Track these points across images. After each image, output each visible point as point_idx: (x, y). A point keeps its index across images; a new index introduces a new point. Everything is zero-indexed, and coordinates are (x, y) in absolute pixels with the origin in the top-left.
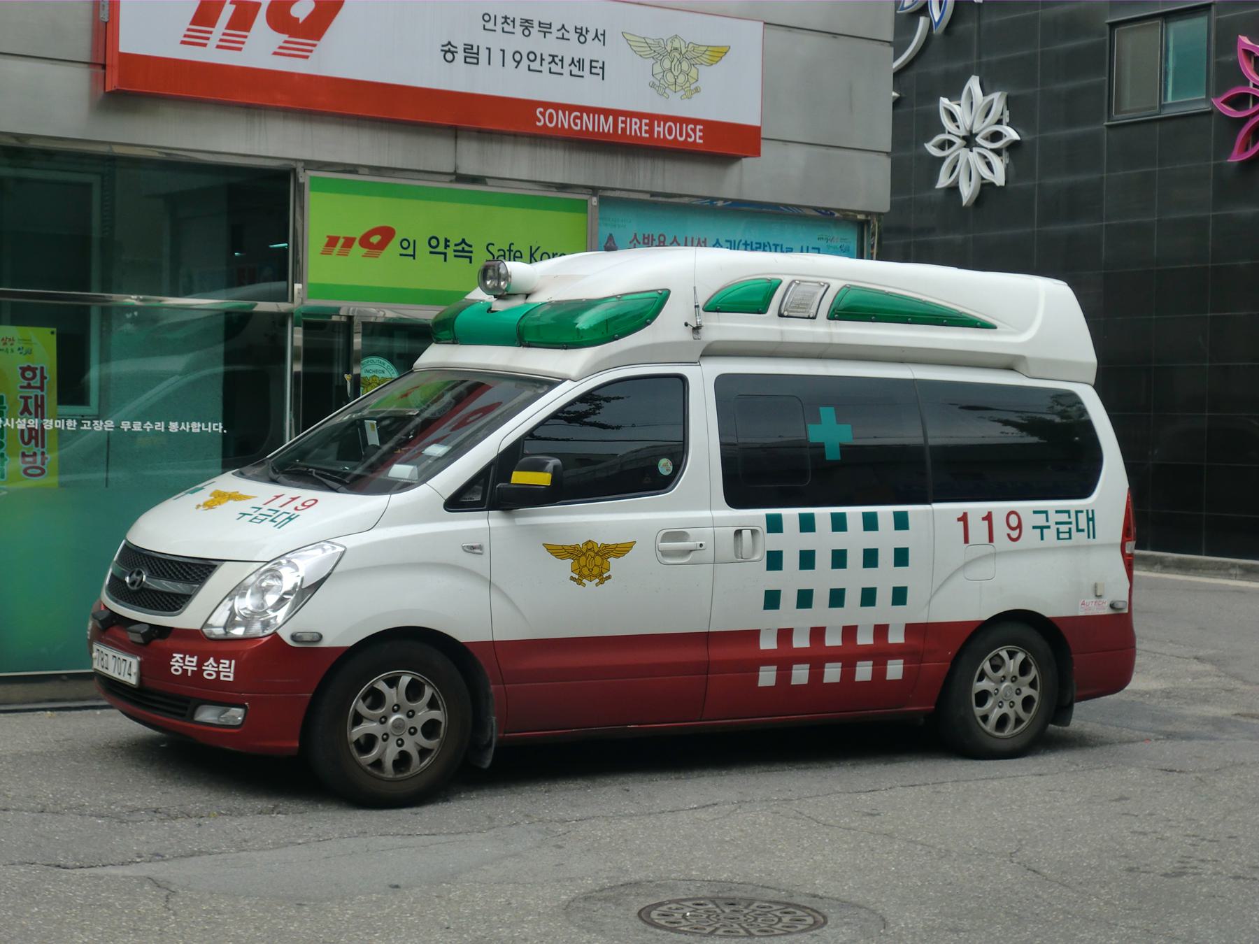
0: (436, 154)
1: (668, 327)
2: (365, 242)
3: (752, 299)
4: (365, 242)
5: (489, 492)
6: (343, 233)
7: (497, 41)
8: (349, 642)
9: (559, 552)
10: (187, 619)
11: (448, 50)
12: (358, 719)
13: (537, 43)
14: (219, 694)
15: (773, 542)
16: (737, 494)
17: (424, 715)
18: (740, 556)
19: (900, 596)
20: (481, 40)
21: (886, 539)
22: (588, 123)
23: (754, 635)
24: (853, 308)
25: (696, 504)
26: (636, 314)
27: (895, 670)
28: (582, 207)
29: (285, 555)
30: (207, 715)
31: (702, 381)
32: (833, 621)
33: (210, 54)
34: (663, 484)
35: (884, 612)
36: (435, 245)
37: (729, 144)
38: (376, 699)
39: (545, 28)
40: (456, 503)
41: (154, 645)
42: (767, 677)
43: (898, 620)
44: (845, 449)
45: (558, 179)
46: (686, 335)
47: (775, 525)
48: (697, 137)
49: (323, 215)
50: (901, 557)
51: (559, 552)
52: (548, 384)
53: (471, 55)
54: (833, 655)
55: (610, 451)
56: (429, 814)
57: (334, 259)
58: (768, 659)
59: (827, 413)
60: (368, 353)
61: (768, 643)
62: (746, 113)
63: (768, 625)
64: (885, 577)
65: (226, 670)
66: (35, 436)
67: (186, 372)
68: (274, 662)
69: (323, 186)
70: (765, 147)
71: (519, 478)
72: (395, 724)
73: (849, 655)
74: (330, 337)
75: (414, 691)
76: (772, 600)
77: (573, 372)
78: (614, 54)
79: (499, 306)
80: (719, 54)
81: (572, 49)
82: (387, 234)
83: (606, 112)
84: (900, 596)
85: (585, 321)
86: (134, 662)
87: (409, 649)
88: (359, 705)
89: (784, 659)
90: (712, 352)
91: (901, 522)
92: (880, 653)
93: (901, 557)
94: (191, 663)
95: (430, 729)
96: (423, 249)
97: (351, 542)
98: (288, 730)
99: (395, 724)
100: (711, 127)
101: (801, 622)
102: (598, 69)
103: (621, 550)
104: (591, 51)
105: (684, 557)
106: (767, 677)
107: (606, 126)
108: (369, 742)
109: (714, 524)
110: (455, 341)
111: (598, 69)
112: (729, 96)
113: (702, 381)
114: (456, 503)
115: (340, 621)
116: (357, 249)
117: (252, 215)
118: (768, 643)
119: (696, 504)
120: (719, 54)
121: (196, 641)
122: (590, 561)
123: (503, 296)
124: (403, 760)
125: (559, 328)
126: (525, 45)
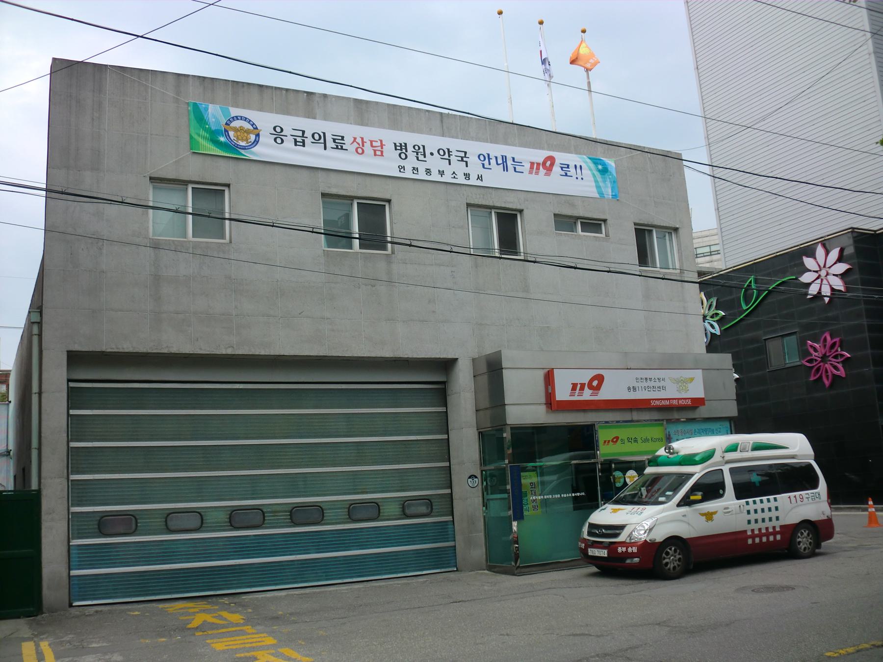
0: (627, 416)
1: (717, 458)
2: (612, 441)
3: (733, 448)
4: (612, 441)
5: (686, 502)
6: (607, 439)
7: (640, 384)
8: (661, 540)
9: (703, 515)
10: (621, 539)
11: (629, 389)
12: (664, 558)
13: (652, 384)
14: (632, 555)
15: (748, 507)
16: (738, 497)
17: (678, 557)
18: (741, 512)
19: (777, 518)
20: (636, 385)
21: (773, 504)
22: (663, 403)
23: (745, 531)
24: (757, 447)
25: (729, 501)
26: (709, 455)
27: (778, 537)
28: (662, 425)
29: (639, 523)
30: (628, 561)
31: (726, 469)
32: (763, 526)
33: (576, 398)
34: (721, 496)
35: (775, 523)
36: (636, 441)
37: (697, 403)
38: (667, 554)
39: (650, 379)
40: (679, 505)
41: (612, 547)
42: (750, 541)
43: (777, 524)
44: (760, 482)
45: (656, 418)
46: (721, 459)
47: (747, 503)
48: (690, 403)
49: (603, 435)
50: (777, 509)
51: (703, 515)
52: (692, 475)
53: (634, 389)
54: (757, 536)
55: (710, 489)
56: (682, 580)
57: (606, 447)
58: (750, 537)
59: (754, 474)
60: (616, 469)
61: (749, 533)
62: (700, 394)
63: (748, 528)
64: (774, 514)
65: (635, 550)
66: (545, 503)
67: (558, 479)
68: (646, 547)
69: (603, 427)
70: (706, 402)
71: (692, 498)
72: (672, 559)
73: (760, 535)
74: (609, 466)
75: (675, 551)
76: (749, 522)
77: (698, 472)
78: (667, 383)
79: (670, 456)
80: (692, 379)
81: (657, 384)
82: (617, 438)
83: (667, 399)
84: (777, 518)
85: (697, 458)
86: (606, 551)
87: (673, 540)
88: (664, 555)
89: (753, 537)
90: (728, 462)
91: (775, 499)
92: (774, 533)
93: (777, 509)
94: (624, 549)
95: (679, 560)
96: (626, 441)
97: (659, 516)
98: (653, 563)
99: (672, 559)
100: (693, 399)
101: (755, 527)
102: (664, 388)
103: (715, 513)
104: (662, 384)
105: (729, 513)
106: (750, 541)
107: (668, 403)
108: (667, 564)
109: (734, 504)
110: (658, 465)
111: (664, 388)
112: (696, 390)
113: (726, 469)
114: (679, 505)
115: (659, 536)
116: (611, 443)
117: (582, 438)
118: (749, 533)
119: (729, 501)
120: (692, 379)
121: (622, 544)
122: (709, 516)
123: (671, 454)
124: (674, 568)
125: (689, 460)
126: (646, 384)
